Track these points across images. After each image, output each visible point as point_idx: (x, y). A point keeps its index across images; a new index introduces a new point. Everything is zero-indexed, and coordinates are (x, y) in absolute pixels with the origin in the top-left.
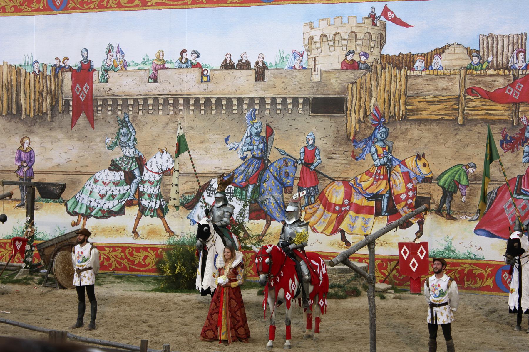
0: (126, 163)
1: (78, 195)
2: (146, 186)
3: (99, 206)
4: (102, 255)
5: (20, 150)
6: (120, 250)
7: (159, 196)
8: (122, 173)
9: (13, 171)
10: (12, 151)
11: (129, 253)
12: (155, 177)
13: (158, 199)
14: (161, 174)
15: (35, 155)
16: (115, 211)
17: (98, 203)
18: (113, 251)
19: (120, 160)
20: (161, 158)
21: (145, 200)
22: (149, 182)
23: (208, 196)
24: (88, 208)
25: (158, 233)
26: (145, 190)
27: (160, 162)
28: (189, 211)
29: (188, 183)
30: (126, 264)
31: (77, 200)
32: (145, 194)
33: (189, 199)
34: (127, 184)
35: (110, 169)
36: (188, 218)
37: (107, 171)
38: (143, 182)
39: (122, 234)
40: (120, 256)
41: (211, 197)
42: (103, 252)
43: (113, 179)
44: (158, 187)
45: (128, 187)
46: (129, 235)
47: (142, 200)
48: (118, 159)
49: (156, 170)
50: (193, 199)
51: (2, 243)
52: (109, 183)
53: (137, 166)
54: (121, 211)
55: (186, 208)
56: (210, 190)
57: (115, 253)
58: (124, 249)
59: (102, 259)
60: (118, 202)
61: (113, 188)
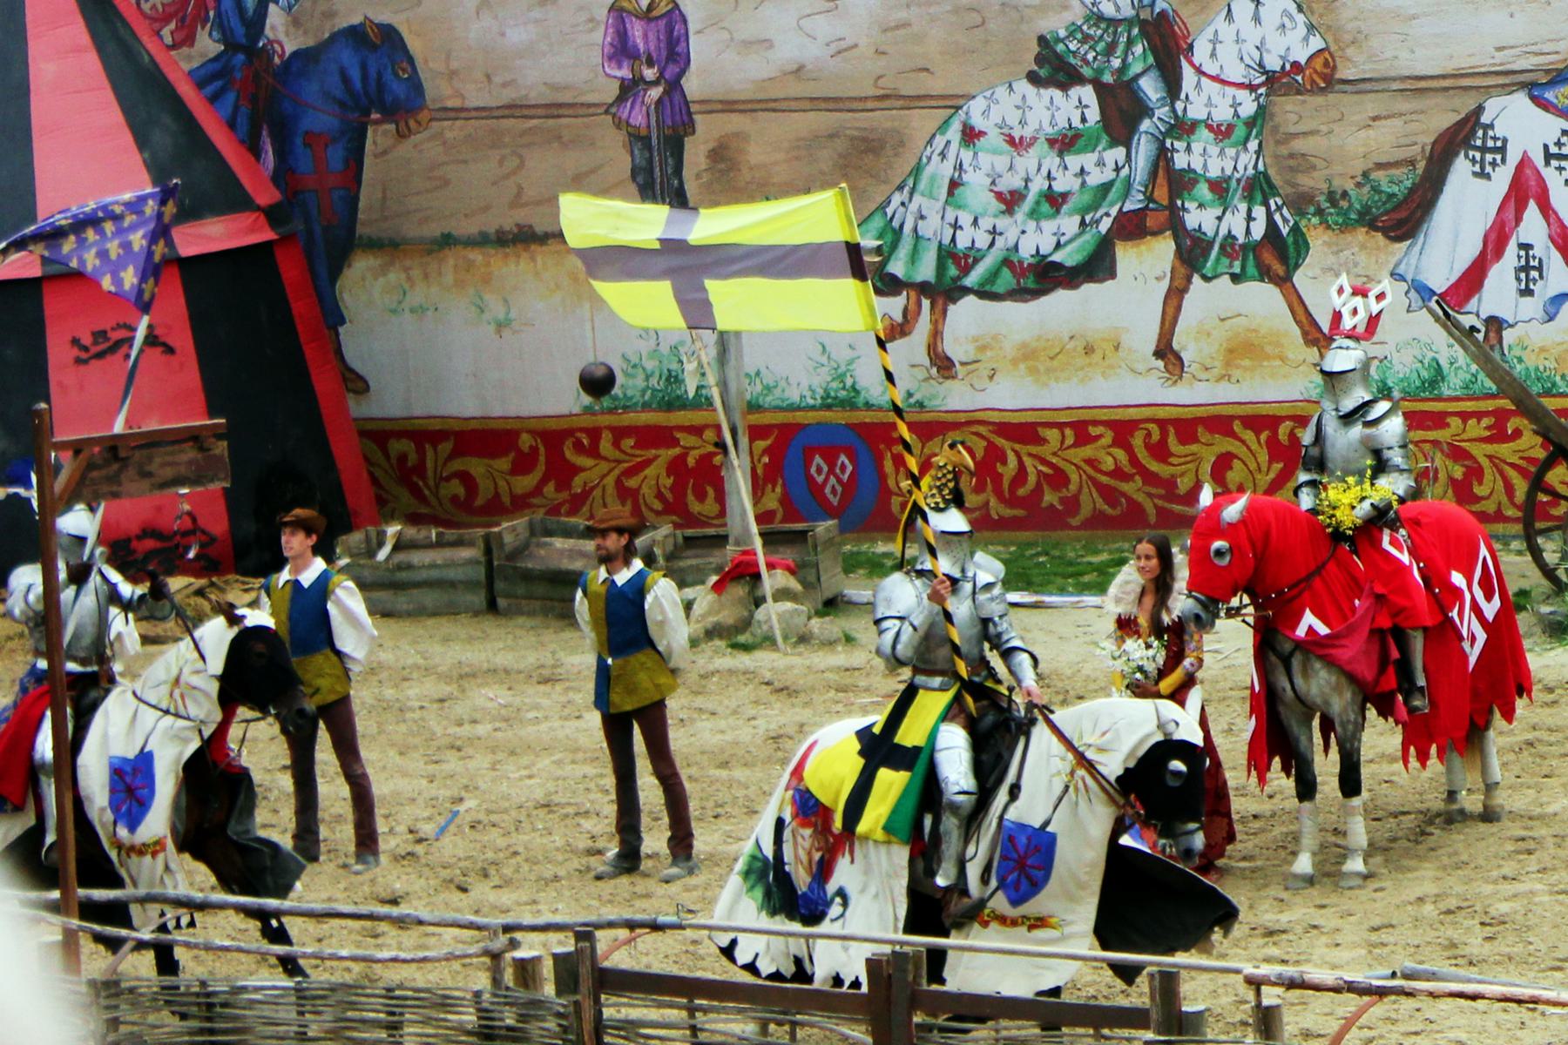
0: (1100, 47)
1: (897, 199)
2: (1197, 147)
3: (1000, 242)
4: (1028, 461)
5: (622, 10)
6: (1108, 438)
7: (1258, 187)
8: (1087, 93)
9: (595, 105)
10: (583, 17)
11: (1149, 447)
12: (1235, 105)
13: (1259, 197)
14: (1262, 90)
15: (692, 27)
16: (1069, 263)
17: (994, 232)
18: (1077, 444)
19: (1071, 35)
20: (1257, 19)
21: (1201, 206)
22: (1210, 128)
23: (1475, 174)
24: (947, 254)
25: (1268, 349)
26: (1197, 165)
27: (1252, 35)
28: (1397, 245)
29: (1383, 122)
30: (1140, 498)
31: (896, 224)
32: (1195, 182)
33: (1394, 195)
34: (1114, 142)
35: (1033, 78)
36: (1396, 276)
37: (1024, 86)
38: (1183, 128)
39: (1111, 367)
40: (1109, 464)
41: (1488, 177)
42: (1034, 449)
43: (1046, 125)
44: (1253, 145)
45: (1120, 153)
46: (1141, 367)
47: (1184, 209)
48: (1062, 33)
49: (1236, 73)
50: (1412, 191)
51: (582, 430)
52: (1034, 139)
53: (1151, 60)
54: (1098, 266)
55: (1385, 232)
56: (1484, 149)
57: (1087, 451)
58: (1123, 430)
59: (1032, 479)
60: (1083, 223)
61: (1052, 161)
